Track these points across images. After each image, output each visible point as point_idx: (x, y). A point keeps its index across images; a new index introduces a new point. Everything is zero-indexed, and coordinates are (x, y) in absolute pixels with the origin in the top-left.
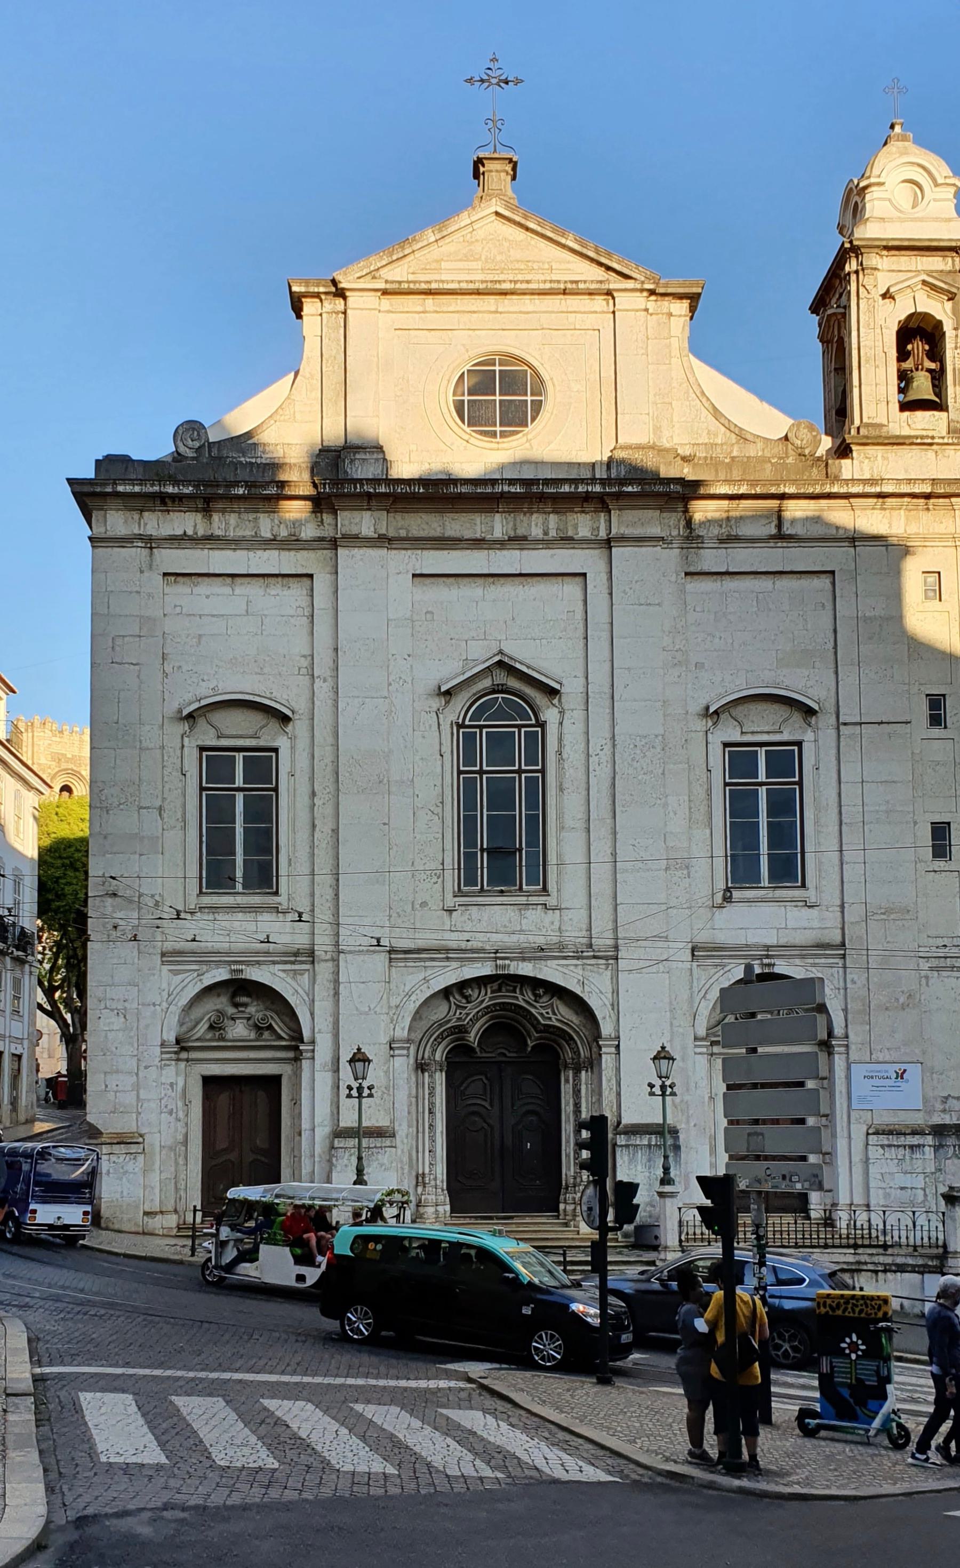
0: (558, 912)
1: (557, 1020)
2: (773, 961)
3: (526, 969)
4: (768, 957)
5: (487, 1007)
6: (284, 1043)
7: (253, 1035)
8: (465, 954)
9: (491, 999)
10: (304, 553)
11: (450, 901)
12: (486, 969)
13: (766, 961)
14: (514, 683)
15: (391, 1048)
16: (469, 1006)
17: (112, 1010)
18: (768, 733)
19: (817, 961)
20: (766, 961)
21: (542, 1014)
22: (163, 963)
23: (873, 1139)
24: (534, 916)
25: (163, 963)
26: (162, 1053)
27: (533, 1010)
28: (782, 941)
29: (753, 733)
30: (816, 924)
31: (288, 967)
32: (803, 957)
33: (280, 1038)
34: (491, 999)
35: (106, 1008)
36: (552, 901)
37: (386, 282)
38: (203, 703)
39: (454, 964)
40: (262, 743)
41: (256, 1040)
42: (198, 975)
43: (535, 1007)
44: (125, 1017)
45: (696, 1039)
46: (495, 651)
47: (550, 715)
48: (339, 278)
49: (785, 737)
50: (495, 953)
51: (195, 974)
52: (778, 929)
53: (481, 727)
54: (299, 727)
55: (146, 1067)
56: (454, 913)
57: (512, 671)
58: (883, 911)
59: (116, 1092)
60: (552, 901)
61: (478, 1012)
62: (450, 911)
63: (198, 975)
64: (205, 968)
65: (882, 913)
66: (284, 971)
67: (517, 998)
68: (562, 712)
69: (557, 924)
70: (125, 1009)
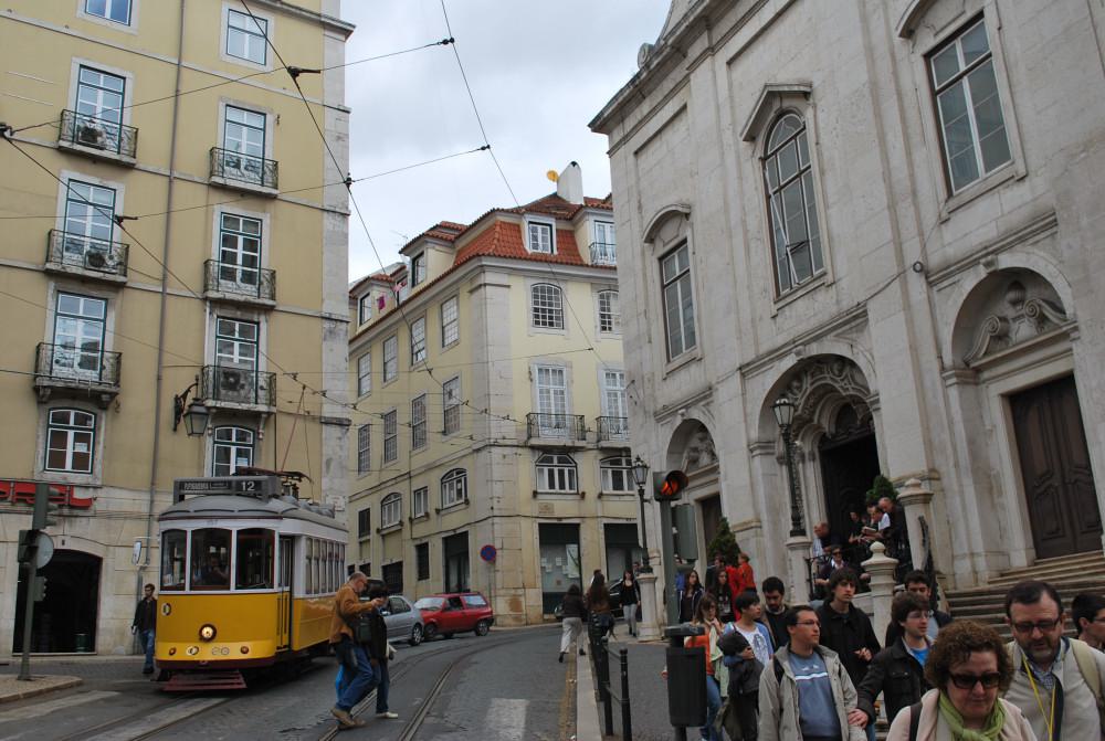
0: (834, 286)
2: (990, 258)
3: (815, 350)
4: (988, 254)
5: (812, 393)
8: (776, 354)
9: (812, 384)
10: (682, 91)
11: (774, 312)
12: (789, 362)
13: (983, 261)
14: (787, 104)
15: (751, 451)
18: (954, 20)
19: (1037, 238)
20: (983, 261)
22: (658, 421)
24: (821, 296)
25: (658, 421)
27: (836, 385)
28: (1002, 229)
29: (942, 29)
30: (1028, 197)
31: (703, 403)
32: (1022, 240)
34: (812, 384)
36: (829, 279)
39: (776, 363)
40: (680, 239)
43: (836, 382)
45: (943, 369)
46: (762, 86)
47: (809, 114)
49: (969, 14)
50: (794, 342)
52: (996, 220)
53: (774, 153)
54: (692, 219)
56: (777, 319)
57: (781, 95)
58: (1081, 148)
60: (829, 279)
61: (808, 398)
62: (774, 317)
65: (1083, 151)
67: (825, 378)
68: (815, 106)
69: (835, 297)
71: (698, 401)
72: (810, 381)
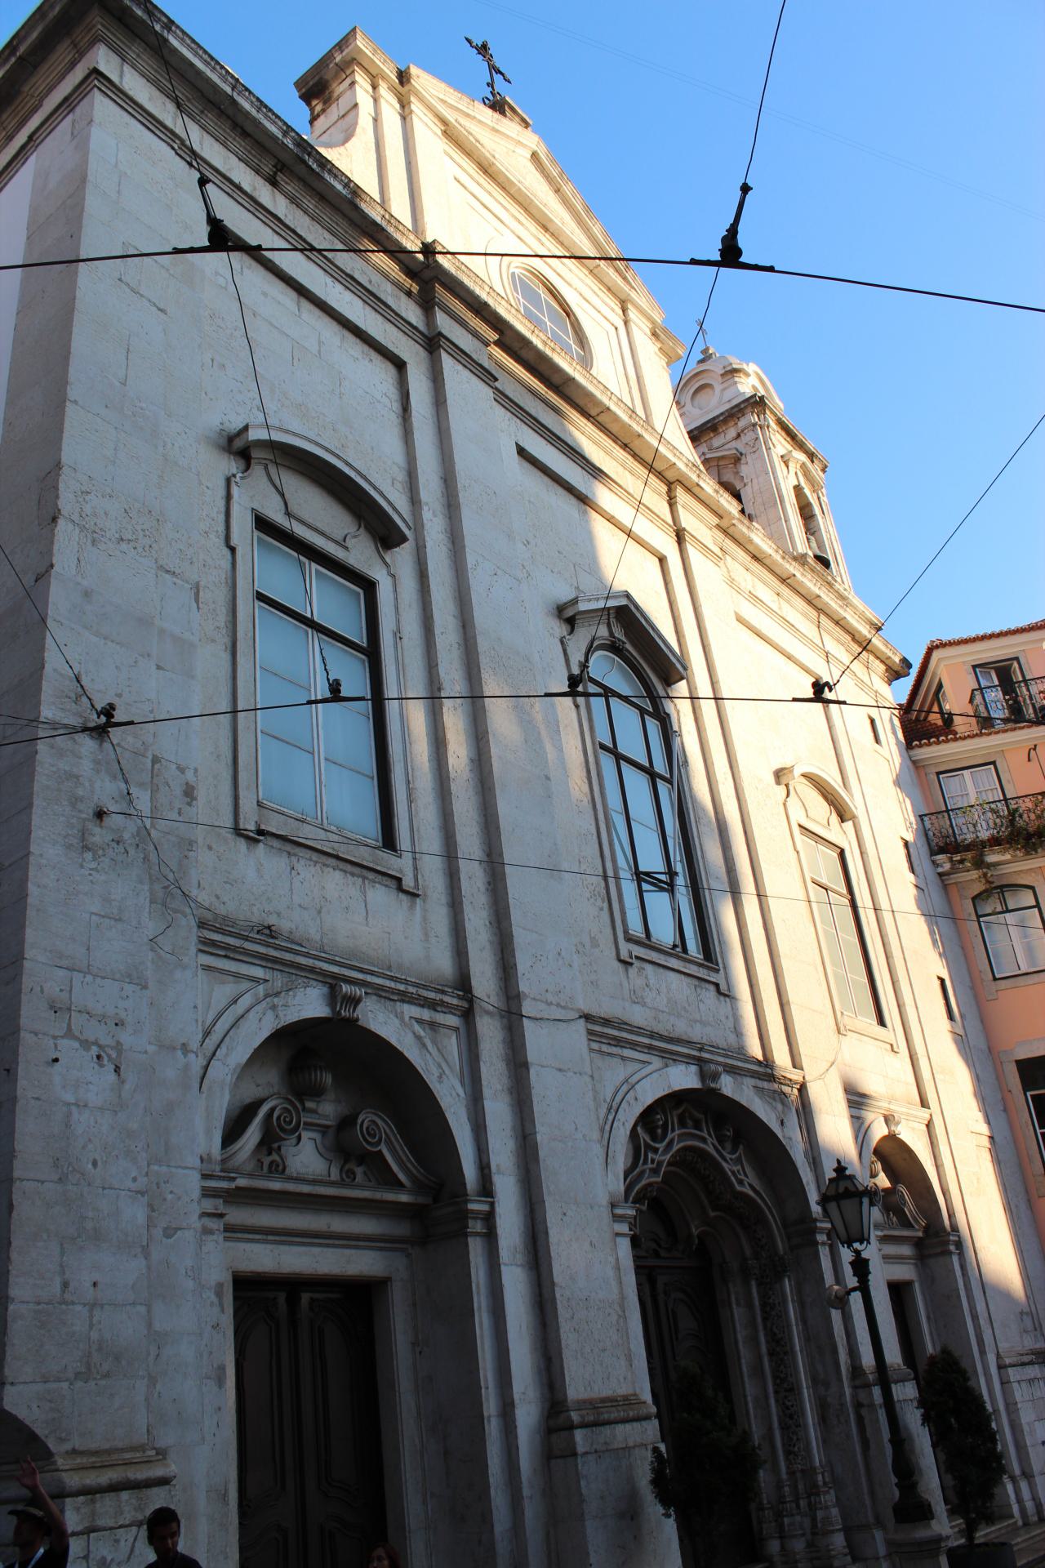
1: (751, 1186)
6: (404, 1198)
7: (335, 1175)
16: (661, 1146)
17: (86, 1044)
21: (733, 1172)
23: (1013, 1374)
26: (207, 1193)
27: (724, 1164)
33: (400, 1185)
35: (69, 1034)
37: (456, 121)
38: (277, 436)
41: (341, 1184)
42: (267, 996)
44: (117, 1070)
48: (414, 70)
51: (261, 989)
55: (169, 1232)
59: (93, 1306)
63: (267, 996)
64: (278, 980)
66: (419, 1021)
70: (118, 1046)
71: (405, 997)
72: (677, 1132)
